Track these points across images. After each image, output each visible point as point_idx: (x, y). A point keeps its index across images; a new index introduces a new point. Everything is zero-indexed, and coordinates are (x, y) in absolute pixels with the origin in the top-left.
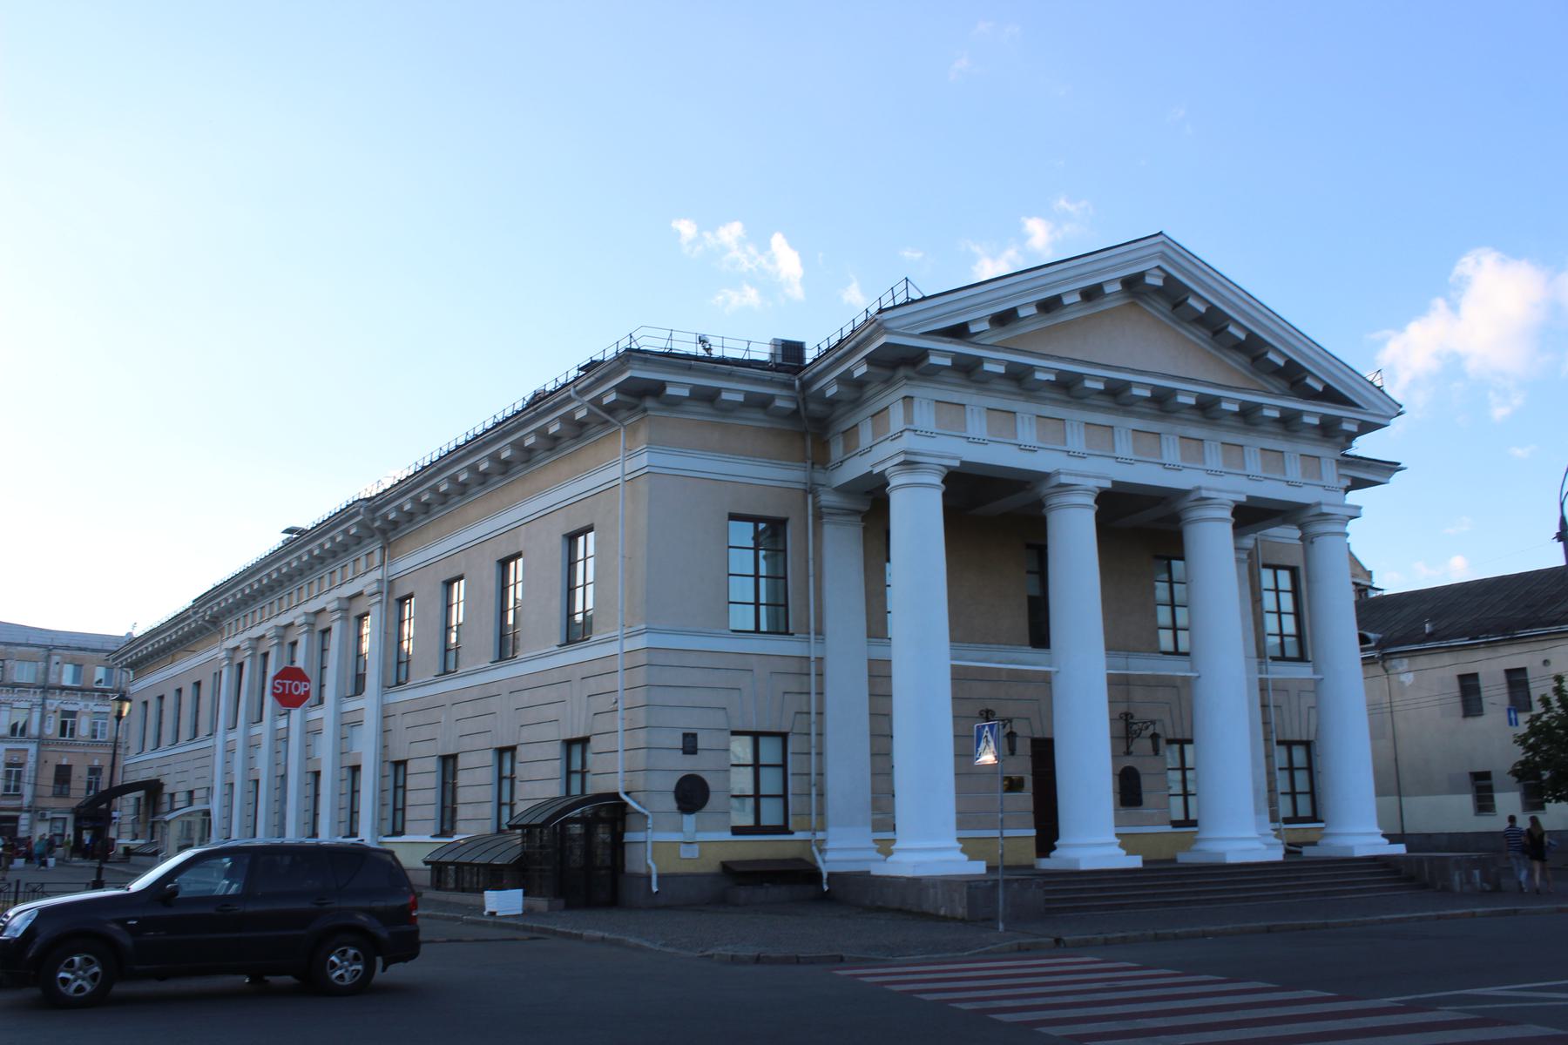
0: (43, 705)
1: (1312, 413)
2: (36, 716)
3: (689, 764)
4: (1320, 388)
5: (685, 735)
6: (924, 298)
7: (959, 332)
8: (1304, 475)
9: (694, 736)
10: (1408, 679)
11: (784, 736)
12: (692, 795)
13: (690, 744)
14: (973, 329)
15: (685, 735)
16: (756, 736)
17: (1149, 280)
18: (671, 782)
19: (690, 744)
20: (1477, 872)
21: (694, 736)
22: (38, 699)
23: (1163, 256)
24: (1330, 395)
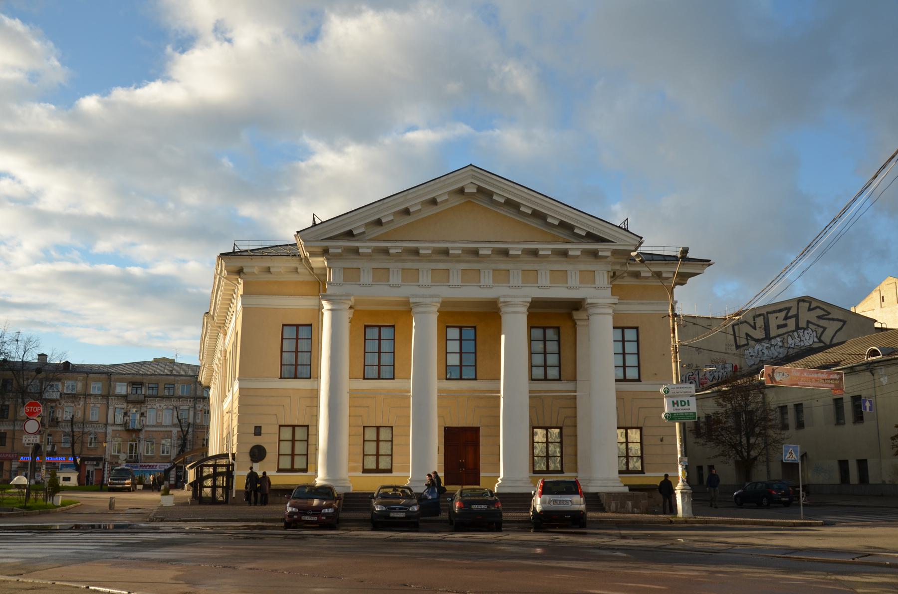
0: (195, 407)
1: (575, 248)
2: (191, 413)
3: (257, 441)
4: (584, 234)
5: (256, 427)
6: (322, 223)
7: (349, 234)
8: (581, 283)
9: (260, 427)
10: (884, 380)
11: (308, 426)
12: (258, 454)
13: (258, 431)
14: (355, 232)
15: (256, 427)
16: (294, 427)
17: (466, 190)
18: (248, 449)
19: (258, 431)
20: (630, 503)
21: (260, 427)
22: (192, 404)
23: (473, 177)
24: (591, 237)
